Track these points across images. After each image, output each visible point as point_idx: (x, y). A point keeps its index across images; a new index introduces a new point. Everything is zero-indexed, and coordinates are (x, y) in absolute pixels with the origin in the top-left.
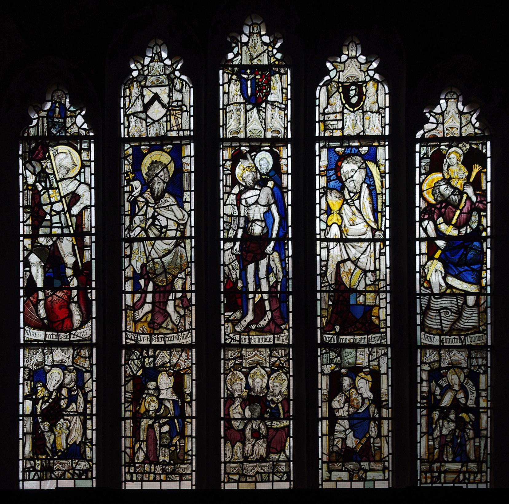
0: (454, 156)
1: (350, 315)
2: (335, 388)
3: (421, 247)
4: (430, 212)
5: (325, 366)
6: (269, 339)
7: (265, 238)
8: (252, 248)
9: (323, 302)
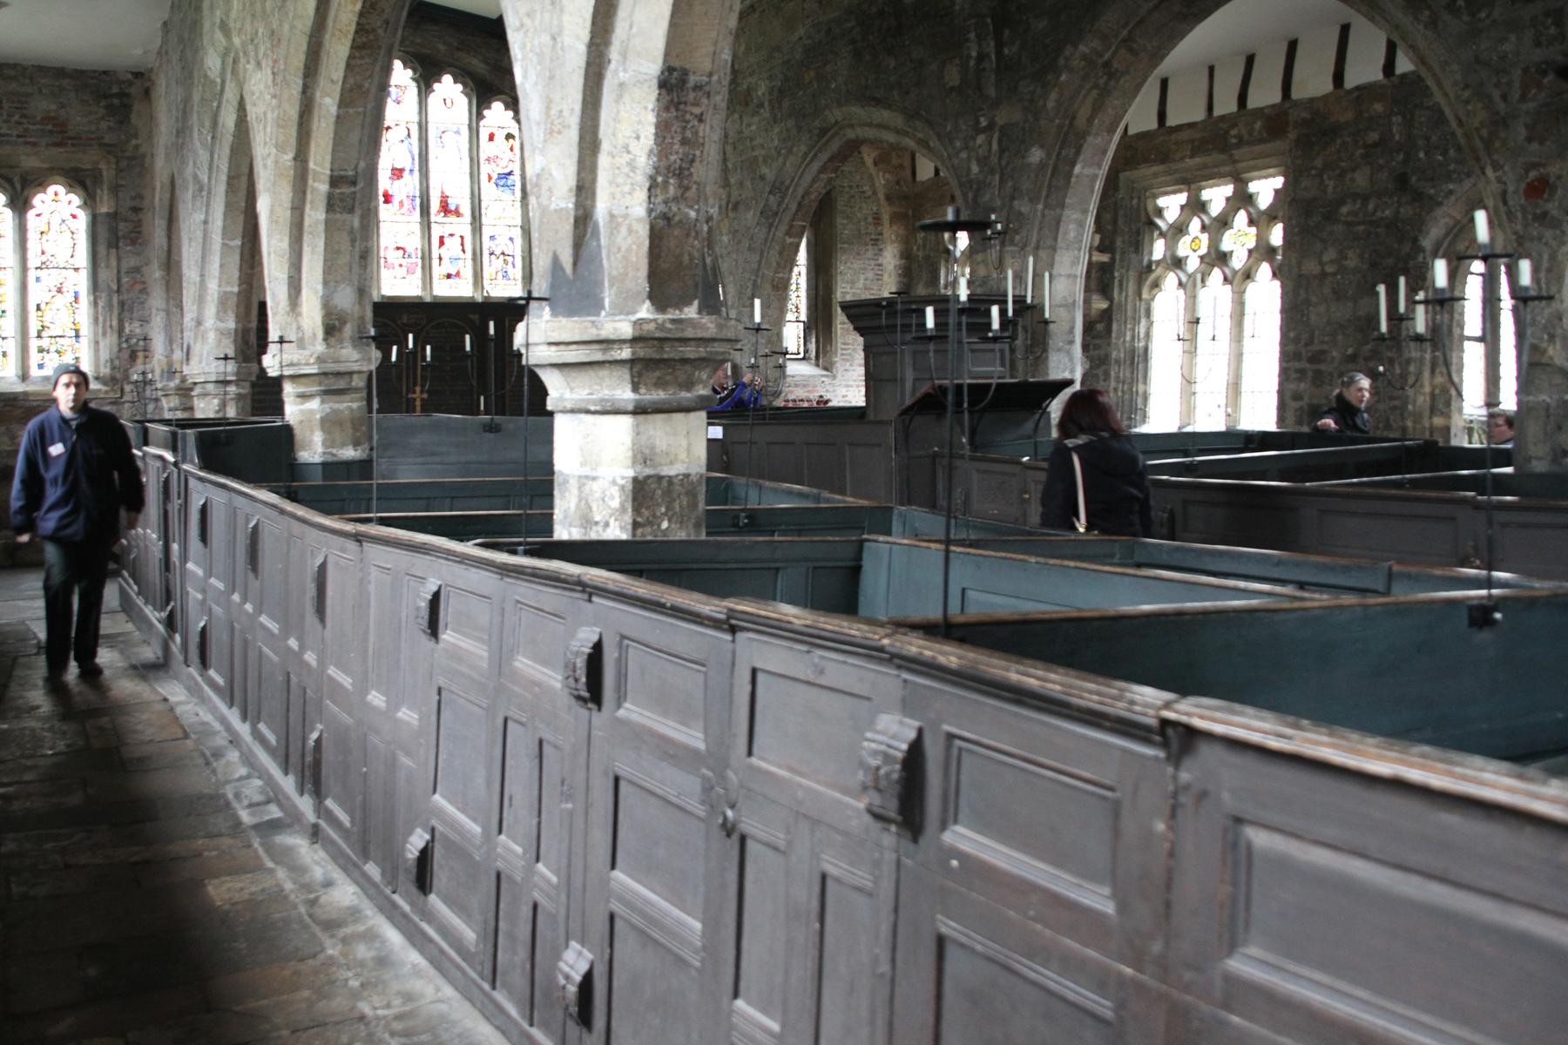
0: (500, 136)
1: (445, 208)
2: (442, 243)
3: (484, 178)
4: (488, 160)
5: (436, 232)
6: (406, 218)
7: (401, 171)
8: (397, 173)
9: (435, 205)
